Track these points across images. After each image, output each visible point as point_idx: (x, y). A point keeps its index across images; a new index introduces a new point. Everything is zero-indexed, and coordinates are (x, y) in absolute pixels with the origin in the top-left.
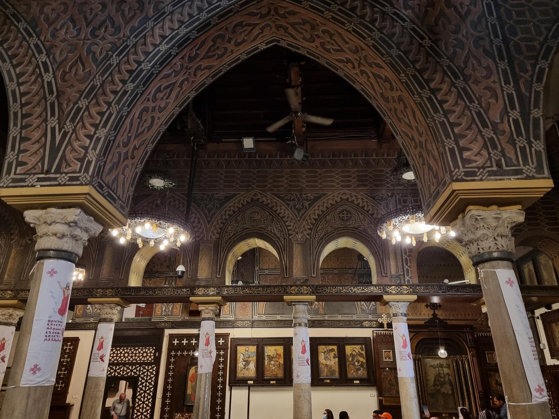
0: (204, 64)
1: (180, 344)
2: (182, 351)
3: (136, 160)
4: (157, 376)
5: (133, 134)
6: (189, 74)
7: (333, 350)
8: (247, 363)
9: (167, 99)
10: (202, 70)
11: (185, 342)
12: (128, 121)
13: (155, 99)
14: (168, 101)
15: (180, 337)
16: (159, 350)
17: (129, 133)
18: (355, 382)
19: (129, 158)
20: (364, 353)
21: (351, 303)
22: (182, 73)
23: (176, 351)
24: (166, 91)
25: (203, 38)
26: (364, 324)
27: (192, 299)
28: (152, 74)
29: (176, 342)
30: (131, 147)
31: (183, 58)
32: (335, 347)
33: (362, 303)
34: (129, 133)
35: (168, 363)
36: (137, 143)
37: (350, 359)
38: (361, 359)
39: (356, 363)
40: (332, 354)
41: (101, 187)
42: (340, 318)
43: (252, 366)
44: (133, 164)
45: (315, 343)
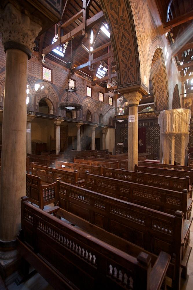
0: (121, 15)
6: (122, 24)
9: (126, 39)
10: (123, 15)
13: (122, 46)
14: (127, 39)
17: (124, 63)
19: (131, 68)
22: (120, 29)
24: (123, 39)
25: (110, 16)
31: (115, 28)
34: (124, 63)
41: (122, 86)
44: (134, 68)
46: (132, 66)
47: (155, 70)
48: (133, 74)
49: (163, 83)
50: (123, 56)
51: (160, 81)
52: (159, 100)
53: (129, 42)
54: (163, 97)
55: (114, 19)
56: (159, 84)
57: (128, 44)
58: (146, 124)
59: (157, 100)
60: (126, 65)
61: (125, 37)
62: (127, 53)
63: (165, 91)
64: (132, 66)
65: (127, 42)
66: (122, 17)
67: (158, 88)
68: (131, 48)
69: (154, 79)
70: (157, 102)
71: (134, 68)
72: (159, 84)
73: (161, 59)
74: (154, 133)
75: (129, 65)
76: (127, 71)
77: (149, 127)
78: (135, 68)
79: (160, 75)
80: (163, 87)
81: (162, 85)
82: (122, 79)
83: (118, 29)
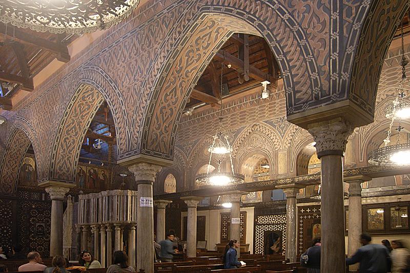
3: (170, 132)
13: (166, 100)
14: (176, 97)
22: (177, 80)
24: (172, 93)
25: (179, 58)
28: (157, 92)
31: (173, 74)
44: (168, 135)
48: (165, 142)
49: (77, 137)
50: (161, 112)
51: (72, 132)
52: (60, 160)
53: (176, 101)
54: (68, 159)
55: (180, 65)
56: (69, 137)
59: (57, 161)
61: (176, 92)
62: (166, 112)
63: (75, 151)
65: (174, 100)
67: (65, 141)
68: (174, 110)
69: (66, 125)
70: (57, 163)
71: (168, 135)
72: (69, 137)
73: (95, 104)
76: (158, 134)
78: (169, 137)
80: (73, 143)
81: (74, 140)
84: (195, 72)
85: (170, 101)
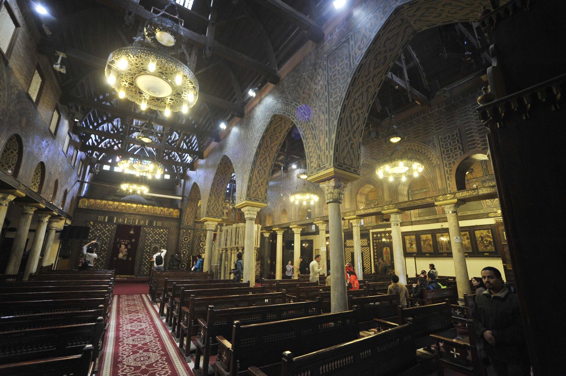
0: (273, 145)
1: (377, 237)
2: (379, 239)
3: (264, 185)
4: (370, 252)
5: (258, 178)
7: (465, 235)
8: (411, 245)
11: (379, 235)
12: (254, 176)
13: (261, 165)
15: (377, 233)
16: (369, 240)
18: (485, 254)
20: (490, 235)
21: (478, 202)
23: (376, 240)
26: (490, 215)
27: (436, 203)
29: (375, 236)
30: (260, 182)
32: (467, 233)
33: (487, 200)
35: (373, 246)
36: (262, 180)
37: (480, 239)
38: (489, 239)
39: (485, 242)
40: (465, 237)
42: (469, 213)
43: (414, 246)
45: (404, 234)
46: (262, 185)
47: (345, 225)
50: (258, 173)
57: (266, 167)
58: (142, 222)
60: (258, 181)
64: (262, 185)
65: (265, 165)
66: (272, 147)
67: (216, 191)
74: (152, 237)
75: (260, 182)
77: (146, 227)
79: (224, 180)
82: (252, 192)
83: (265, 152)
84: (276, 147)
85: (263, 166)
